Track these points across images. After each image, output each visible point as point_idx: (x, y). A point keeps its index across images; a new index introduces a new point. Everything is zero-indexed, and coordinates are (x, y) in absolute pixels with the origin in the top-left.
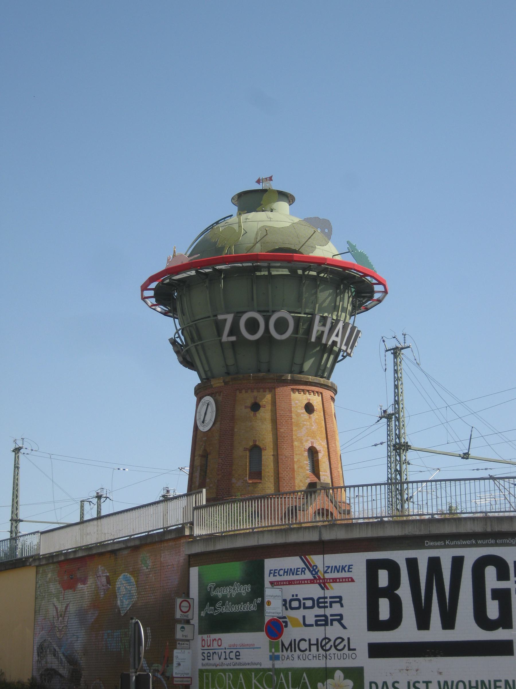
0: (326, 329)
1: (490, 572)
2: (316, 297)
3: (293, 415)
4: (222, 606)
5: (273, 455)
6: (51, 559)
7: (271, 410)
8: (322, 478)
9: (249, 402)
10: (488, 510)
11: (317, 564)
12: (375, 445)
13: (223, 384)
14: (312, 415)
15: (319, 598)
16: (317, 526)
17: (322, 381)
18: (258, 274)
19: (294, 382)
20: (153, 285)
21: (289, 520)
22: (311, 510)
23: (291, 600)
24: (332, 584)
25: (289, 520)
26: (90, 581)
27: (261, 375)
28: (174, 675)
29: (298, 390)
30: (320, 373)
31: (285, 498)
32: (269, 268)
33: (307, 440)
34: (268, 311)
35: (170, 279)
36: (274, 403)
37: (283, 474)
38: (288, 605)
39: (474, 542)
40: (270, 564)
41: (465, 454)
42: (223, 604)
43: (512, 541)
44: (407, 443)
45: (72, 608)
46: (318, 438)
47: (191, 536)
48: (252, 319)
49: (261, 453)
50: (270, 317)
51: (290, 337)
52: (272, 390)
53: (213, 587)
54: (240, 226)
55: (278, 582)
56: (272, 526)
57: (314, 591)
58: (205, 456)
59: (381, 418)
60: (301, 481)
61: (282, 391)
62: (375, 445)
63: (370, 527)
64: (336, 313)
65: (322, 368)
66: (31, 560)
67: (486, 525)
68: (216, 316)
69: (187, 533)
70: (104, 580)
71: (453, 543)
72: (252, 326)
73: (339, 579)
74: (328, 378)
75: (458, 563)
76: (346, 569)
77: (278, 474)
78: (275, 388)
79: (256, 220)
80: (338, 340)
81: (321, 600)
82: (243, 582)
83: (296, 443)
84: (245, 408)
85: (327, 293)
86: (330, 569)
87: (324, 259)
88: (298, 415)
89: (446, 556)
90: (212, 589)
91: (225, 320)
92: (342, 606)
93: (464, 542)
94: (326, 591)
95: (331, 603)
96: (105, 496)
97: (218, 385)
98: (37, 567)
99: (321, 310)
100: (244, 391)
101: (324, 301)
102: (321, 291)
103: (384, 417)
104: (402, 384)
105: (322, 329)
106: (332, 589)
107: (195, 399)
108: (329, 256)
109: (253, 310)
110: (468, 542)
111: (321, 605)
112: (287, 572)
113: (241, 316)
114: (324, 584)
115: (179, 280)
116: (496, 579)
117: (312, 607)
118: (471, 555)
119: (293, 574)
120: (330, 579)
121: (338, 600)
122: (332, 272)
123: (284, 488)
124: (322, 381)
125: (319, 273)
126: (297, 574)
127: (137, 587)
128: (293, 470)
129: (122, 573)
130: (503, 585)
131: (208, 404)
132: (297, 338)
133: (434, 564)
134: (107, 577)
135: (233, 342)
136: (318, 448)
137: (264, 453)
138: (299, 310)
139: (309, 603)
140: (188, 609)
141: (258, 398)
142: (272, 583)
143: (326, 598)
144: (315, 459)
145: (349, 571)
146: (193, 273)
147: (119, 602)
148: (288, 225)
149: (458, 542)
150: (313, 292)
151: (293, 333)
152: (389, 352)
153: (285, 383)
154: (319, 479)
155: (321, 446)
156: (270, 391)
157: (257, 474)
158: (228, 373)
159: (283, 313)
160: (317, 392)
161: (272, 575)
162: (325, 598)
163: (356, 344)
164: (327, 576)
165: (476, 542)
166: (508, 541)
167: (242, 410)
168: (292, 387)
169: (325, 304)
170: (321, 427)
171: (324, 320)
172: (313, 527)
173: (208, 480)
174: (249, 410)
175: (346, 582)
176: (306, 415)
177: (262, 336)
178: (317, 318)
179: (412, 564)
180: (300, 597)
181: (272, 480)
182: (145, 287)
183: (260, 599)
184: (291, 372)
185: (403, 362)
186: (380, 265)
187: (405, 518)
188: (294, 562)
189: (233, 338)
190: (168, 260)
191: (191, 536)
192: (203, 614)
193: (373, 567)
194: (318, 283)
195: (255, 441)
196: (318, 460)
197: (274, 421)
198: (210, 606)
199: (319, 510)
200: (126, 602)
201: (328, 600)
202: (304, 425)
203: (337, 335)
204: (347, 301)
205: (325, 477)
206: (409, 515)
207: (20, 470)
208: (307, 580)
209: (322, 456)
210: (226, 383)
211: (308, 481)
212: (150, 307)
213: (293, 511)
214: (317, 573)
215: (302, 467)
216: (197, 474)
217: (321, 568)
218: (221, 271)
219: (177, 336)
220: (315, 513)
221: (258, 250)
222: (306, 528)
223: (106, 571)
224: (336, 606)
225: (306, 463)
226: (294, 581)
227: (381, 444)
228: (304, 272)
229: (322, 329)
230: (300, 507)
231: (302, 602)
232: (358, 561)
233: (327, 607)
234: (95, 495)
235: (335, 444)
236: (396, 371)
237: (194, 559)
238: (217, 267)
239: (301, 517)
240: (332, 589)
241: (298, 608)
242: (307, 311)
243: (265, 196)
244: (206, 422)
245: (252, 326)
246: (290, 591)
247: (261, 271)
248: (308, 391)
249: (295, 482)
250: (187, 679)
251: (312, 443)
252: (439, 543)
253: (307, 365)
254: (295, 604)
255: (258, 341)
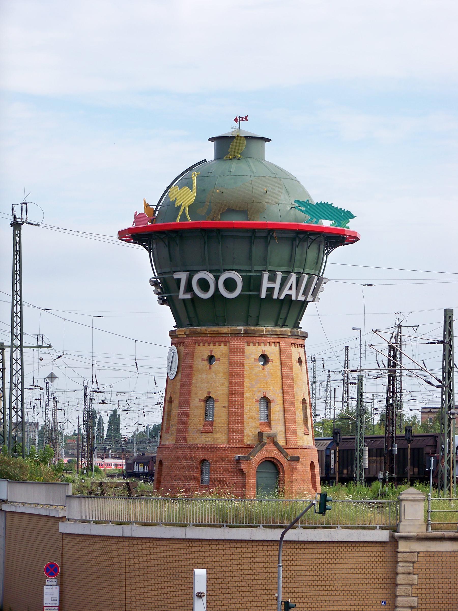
0: (276, 286)
3: (245, 367)
9: (206, 355)
28: (45, 605)
51: (240, 294)
84: (202, 361)
100: (201, 344)
128: (242, 421)
141: (213, 352)
151: (242, 291)
154: (270, 426)
155: (275, 394)
167: (200, 363)
178: (266, 275)
203: (291, 288)
229: (271, 285)
235: (293, 391)
245: (204, 285)
250: (55, 608)
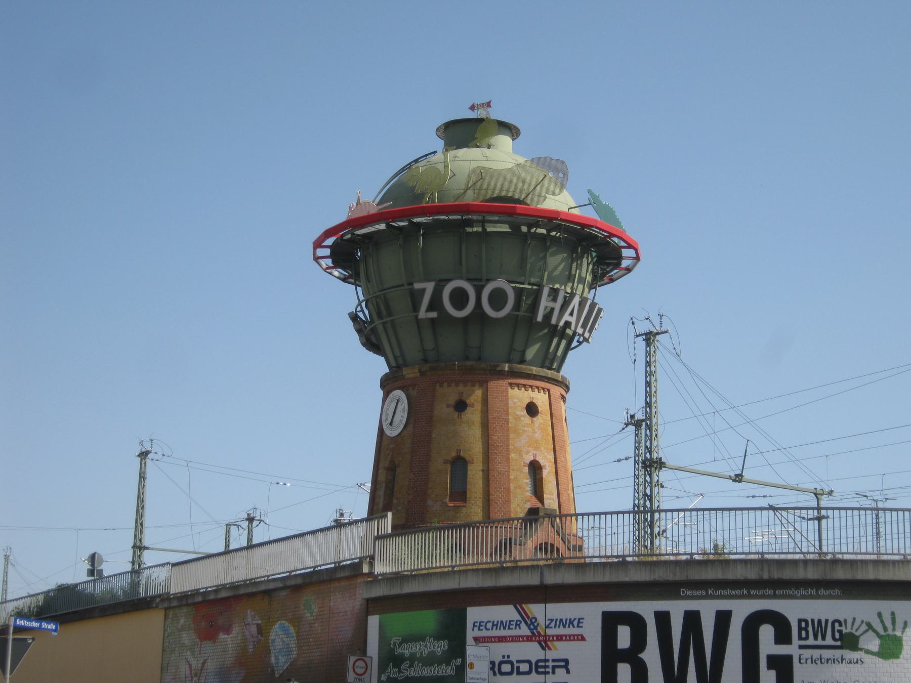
0: (557, 306)
1: (766, 632)
2: (545, 262)
4: (410, 667)
5: (483, 471)
6: (187, 600)
7: (482, 411)
8: (546, 502)
9: (452, 399)
10: (765, 550)
11: (536, 615)
12: (619, 461)
13: (418, 374)
14: (535, 419)
15: (538, 661)
16: (538, 566)
17: (550, 373)
18: (469, 230)
19: (514, 374)
20: (330, 241)
21: (501, 556)
22: (530, 544)
23: (501, 663)
24: (555, 643)
25: (501, 556)
26: (236, 630)
27: (469, 363)
29: (518, 385)
30: (547, 363)
31: (496, 527)
32: (483, 223)
33: (528, 452)
34: (481, 280)
35: (352, 234)
36: (485, 401)
37: (495, 495)
38: (496, 669)
39: (745, 592)
40: (474, 614)
41: (737, 476)
42: (411, 666)
43: (796, 592)
44: (661, 459)
45: (211, 666)
46: (542, 449)
47: (371, 574)
48: (460, 289)
49: (467, 468)
50: (483, 287)
51: (509, 314)
52: (483, 384)
53: (398, 642)
54: (446, 167)
55: (484, 638)
56: (478, 564)
57: (533, 651)
58: (392, 469)
59: (627, 425)
60: (518, 505)
61: (495, 385)
62: (619, 461)
63: (608, 568)
64: (570, 285)
65: (550, 356)
66: (158, 600)
67: (762, 570)
68: (411, 284)
69: (366, 569)
70: (254, 629)
71: (718, 593)
72: (459, 298)
73: (566, 636)
74: (558, 370)
75: (723, 619)
76: (575, 623)
77: (489, 495)
78: (487, 382)
79: (468, 159)
80: (573, 320)
81: (540, 664)
82: (438, 637)
83: (513, 455)
85: (560, 257)
86: (553, 623)
87: (557, 213)
88: (517, 418)
89: (708, 610)
90: (397, 646)
91: (424, 290)
92: (568, 672)
93: (733, 592)
94: (547, 651)
95: (554, 668)
96: (258, 518)
97: (412, 375)
98: (166, 609)
99: (551, 280)
100: (445, 385)
101: (556, 268)
102: (553, 254)
103: (631, 424)
104: (656, 380)
105: (551, 304)
106: (556, 649)
107: (381, 393)
108: (563, 208)
109: (461, 278)
110: (738, 592)
111: (540, 670)
112: (497, 625)
113: (444, 286)
114: (545, 642)
115: (364, 236)
116: (773, 641)
117: (529, 672)
118: (742, 609)
119: (504, 628)
120: (553, 636)
121: (563, 664)
122: (566, 230)
123: (496, 514)
124: (550, 373)
125: (549, 231)
126: (509, 628)
127: (298, 640)
129: (277, 621)
130: (782, 650)
131: (398, 401)
132: (517, 316)
133: (692, 620)
134: (258, 626)
135: (432, 320)
136: (542, 462)
137: (470, 467)
138: (522, 279)
139: (524, 667)
140: (363, 670)
142: (476, 639)
143: (548, 661)
144: (538, 477)
145: (578, 626)
146: (383, 226)
147: (273, 658)
148: (510, 166)
149: (725, 592)
150: (541, 255)
152: (641, 338)
153: (501, 375)
154: (543, 503)
155: (546, 461)
156: (481, 386)
157: (460, 494)
158: (425, 360)
159: (501, 283)
160: (543, 389)
161: (476, 629)
162: (546, 661)
163: (596, 326)
164: (549, 632)
165: (749, 592)
166: (791, 592)
167: (443, 409)
168: (510, 381)
169: (557, 273)
170: (548, 435)
171: (554, 293)
172: (532, 567)
173: (395, 501)
174: (452, 410)
175: (574, 640)
176: (527, 419)
177: (472, 313)
178: (546, 291)
179: (663, 619)
180: (513, 659)
181: (480, 503)
182: (318, 244)
183: (459, 660)
184: (509, 361)
185: (657, 351)
186: (631, 223)
187: (655, 559)
188: (507, 612)
189: (434, 315)
190: (350, 209)
191: (371, 574)
192: (383, 678)
193: (610, 622)
194: (548, 244)
195: (459, 451)
196: (542, 478)
197: (485, 426)
198: (394, 667)
199: (541, 545)
200: (282, 659)
201: (550, 664)
202: (524, 431)
203: (571, 314)
204: (585, 269)
205: (551, 501)
206: (660, 555)
207: (147, 481)
208: (523, 637)
209: (548, 474)
210: (422, 373)
211: (528, 506)
212: (325, 270)
213: (507, 545)
214: (536, 628)
215: (520, 488)
216: (381, 493)
217: (541, 621)
218: (419, 225)
219: (359, 309)
220: (536, 548)
221: (469, 198)
222: (523, 567)
223: (257, 617)
224: (560, 672)
225: (526, 482)
226: (505, 637)
227: (626, 459)
228: (529, 230)
229: (551, 304)
230: (516, 540)
231: (516, 665)
232: (591, 613)
233: (548, 673)
234: (246, 516)
235: (565, 457)
236: (648, 364)
237: (373, 605)
238: (415, 220)
239: (517, 553)
240: (556, 649)
241: (511, 673)
242: (533, 280)
243: (481, 127)
244: (395, 424)
245: (459, 298)
246: (499, 651)
247: (472, 226)
248: (531, 387)
249: (510, 507)
251: (535, 455)
252: (699, 593)
253: (531, 353)
254: (506, 668)
255: (465, 320)
